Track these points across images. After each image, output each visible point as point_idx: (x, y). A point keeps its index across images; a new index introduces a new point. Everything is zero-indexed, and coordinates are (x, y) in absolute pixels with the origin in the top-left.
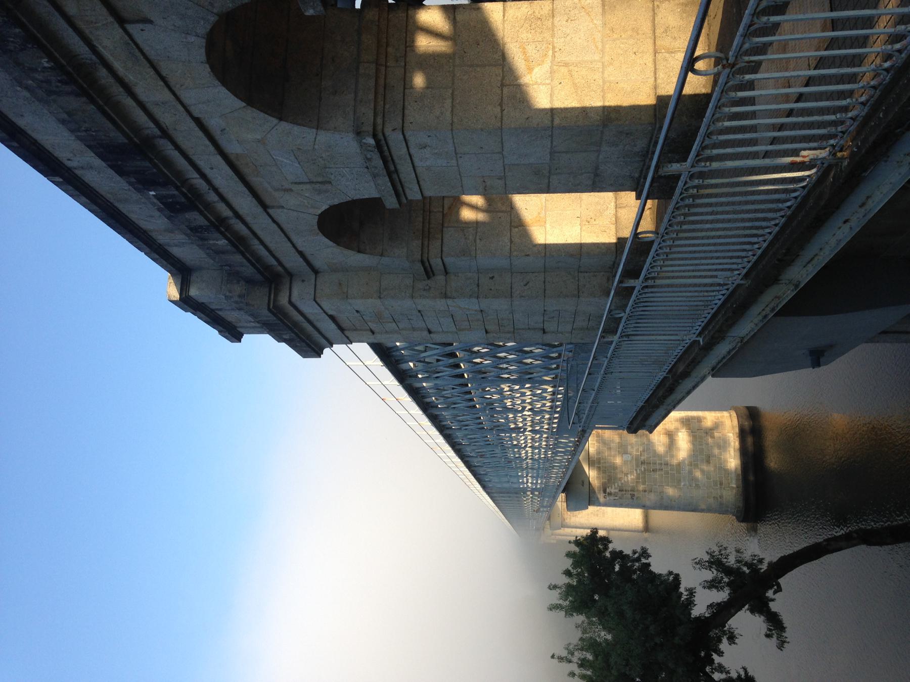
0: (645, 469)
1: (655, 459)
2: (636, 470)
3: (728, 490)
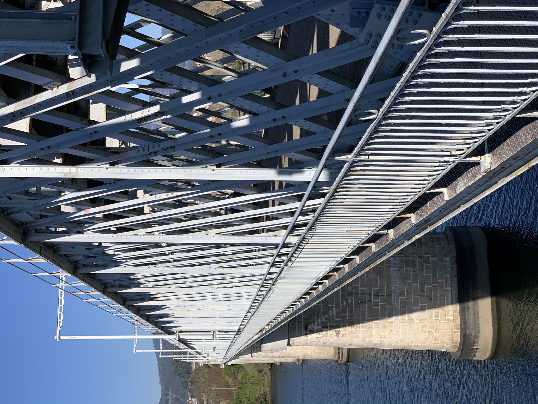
3: (445, 323)
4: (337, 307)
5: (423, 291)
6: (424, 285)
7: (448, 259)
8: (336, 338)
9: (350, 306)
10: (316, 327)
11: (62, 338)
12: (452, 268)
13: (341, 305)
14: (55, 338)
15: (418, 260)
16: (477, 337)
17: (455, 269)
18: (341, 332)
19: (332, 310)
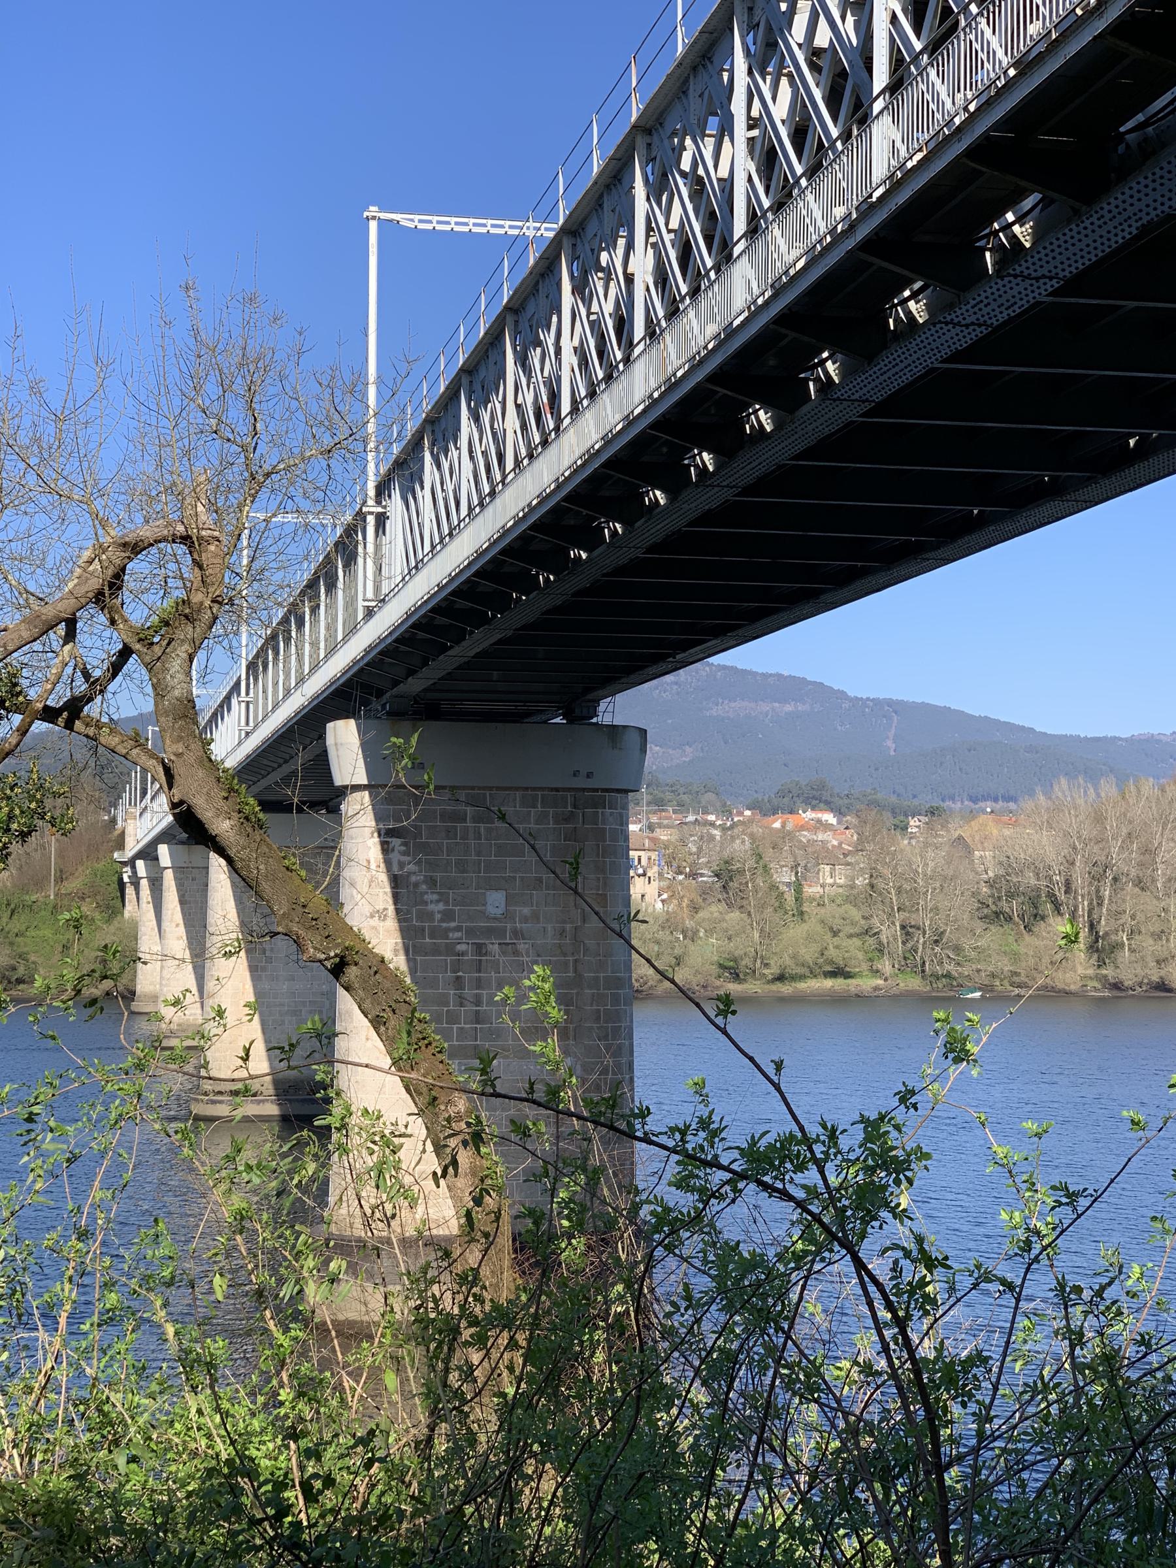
0: (463, 954)
1: (494, 985)
4: (448, 916)
8: (367, 910)
9: (450, 950)
10: (395, 857)
11: (373, 225)
13: (453, 924)
14: (372, 208)
18: (382, 924)
19: (438, 901)
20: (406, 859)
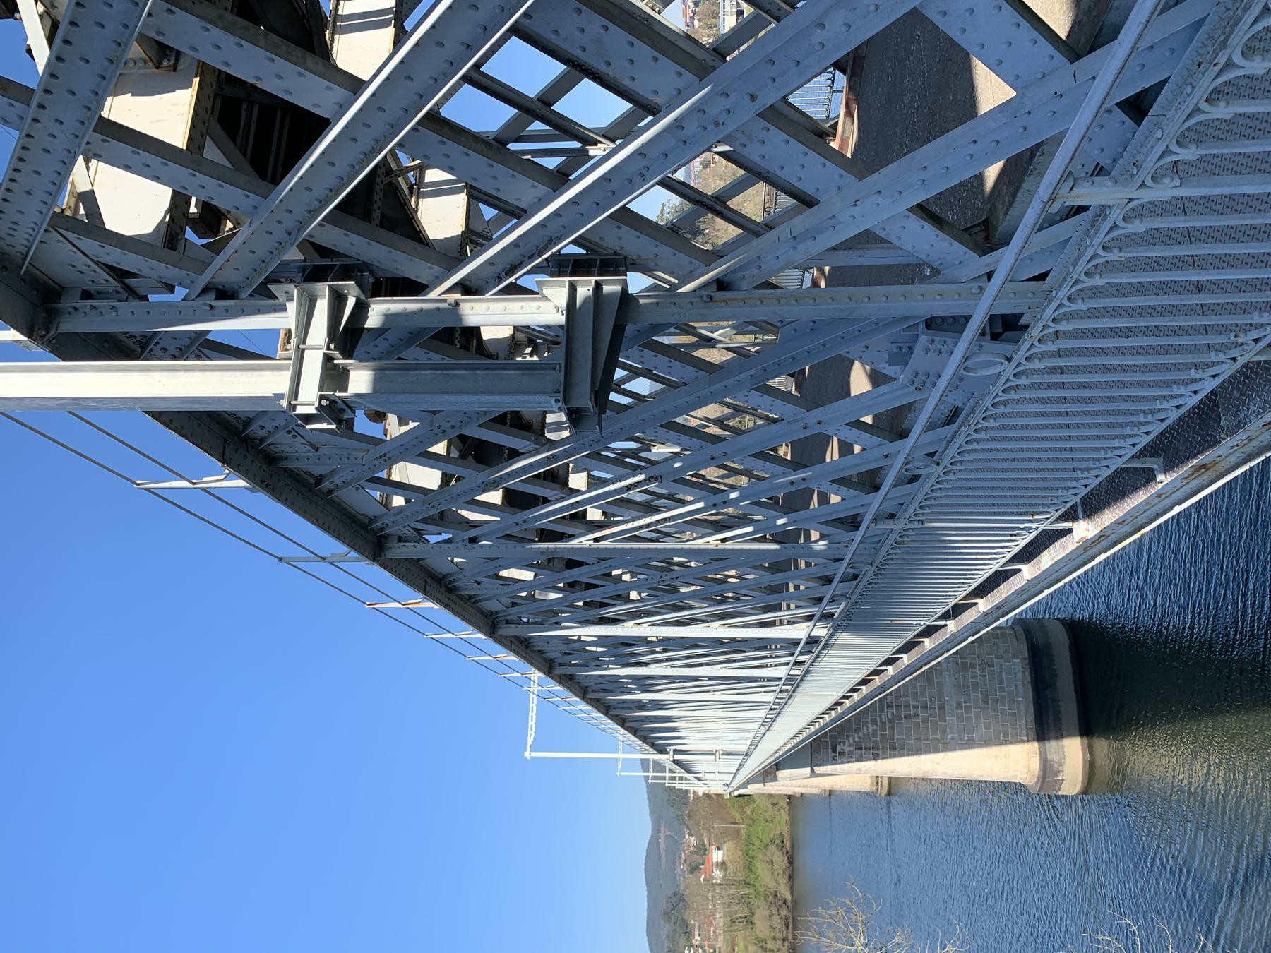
1: (907, 699)
2: (880, 716)
4: (874, 722)
5: (986, 702)
6: (987, 695)
7: (1018, 660)
9: (891, 721)
12: (1023, 672)
13: (878, 720)
15: (978, 662)
16: (1061, 764)
17: (1027, 674)
20: (847, 743)
